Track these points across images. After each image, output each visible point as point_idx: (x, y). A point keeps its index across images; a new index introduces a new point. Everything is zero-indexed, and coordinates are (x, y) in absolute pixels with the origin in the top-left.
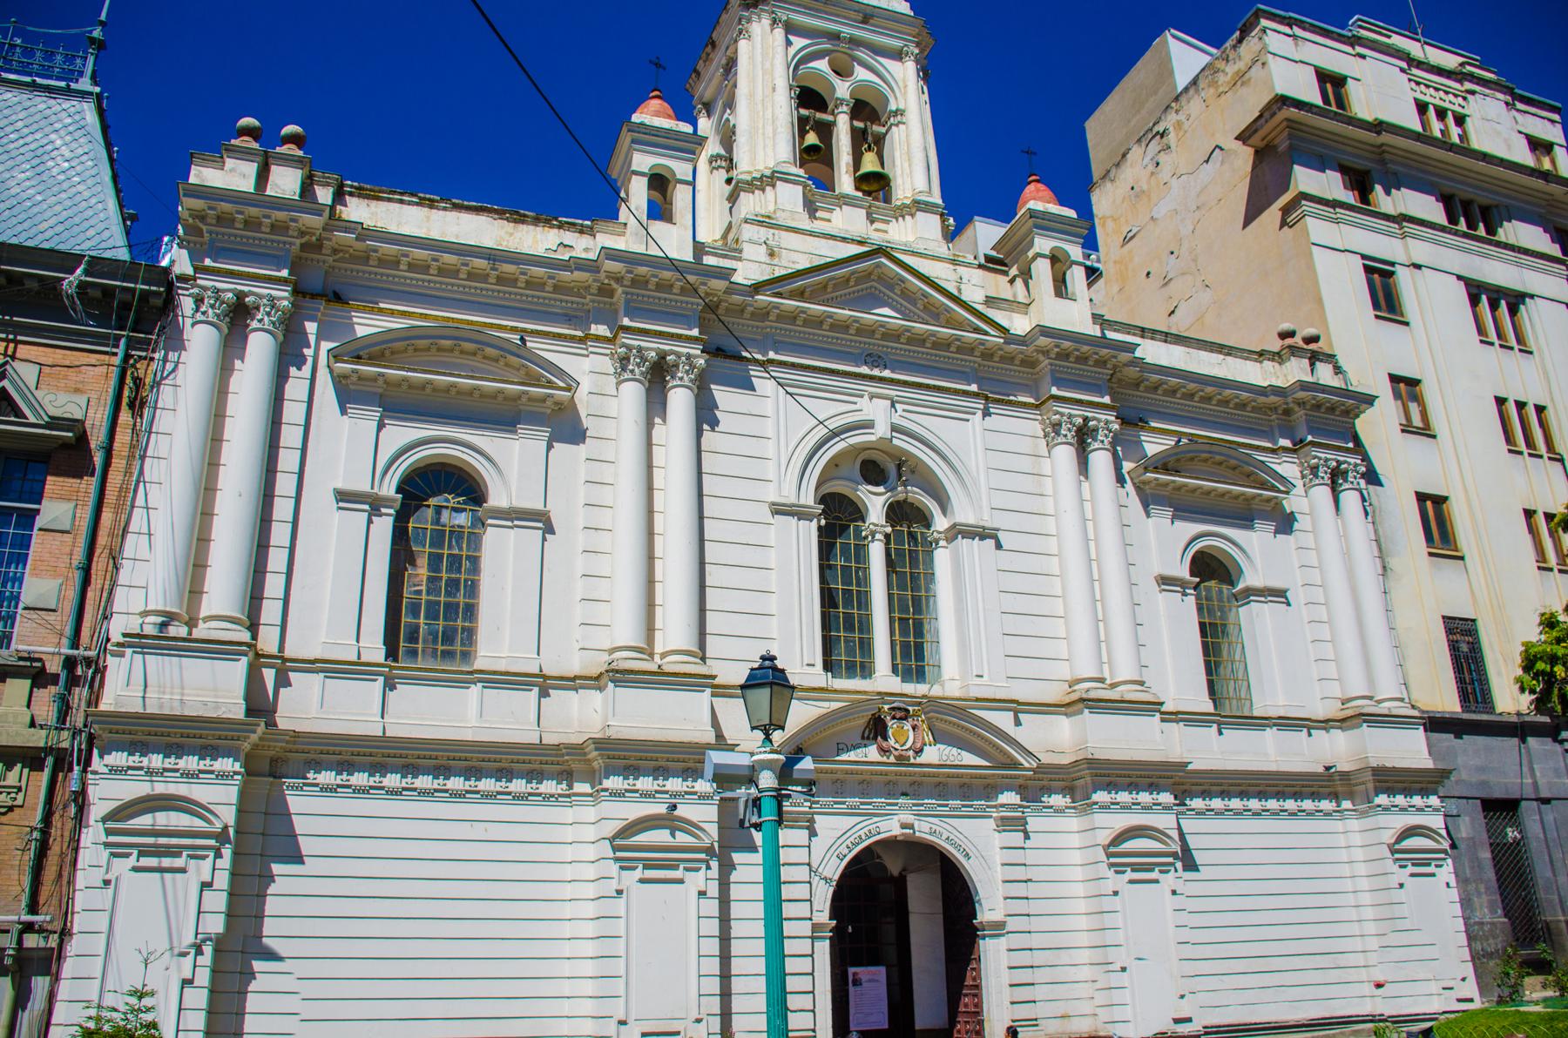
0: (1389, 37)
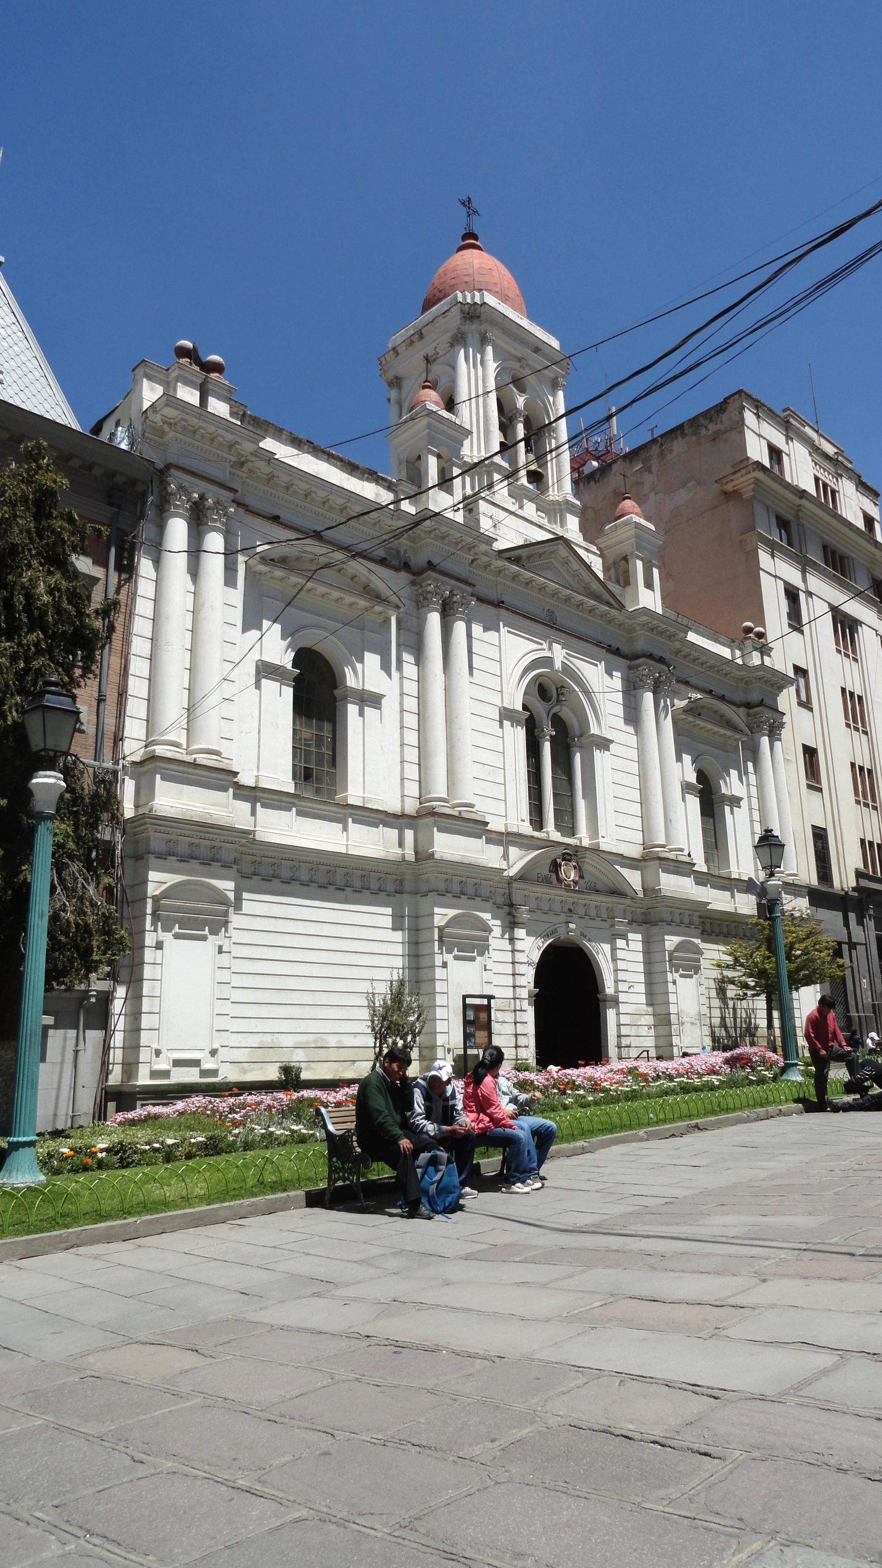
0: (804, 427)
